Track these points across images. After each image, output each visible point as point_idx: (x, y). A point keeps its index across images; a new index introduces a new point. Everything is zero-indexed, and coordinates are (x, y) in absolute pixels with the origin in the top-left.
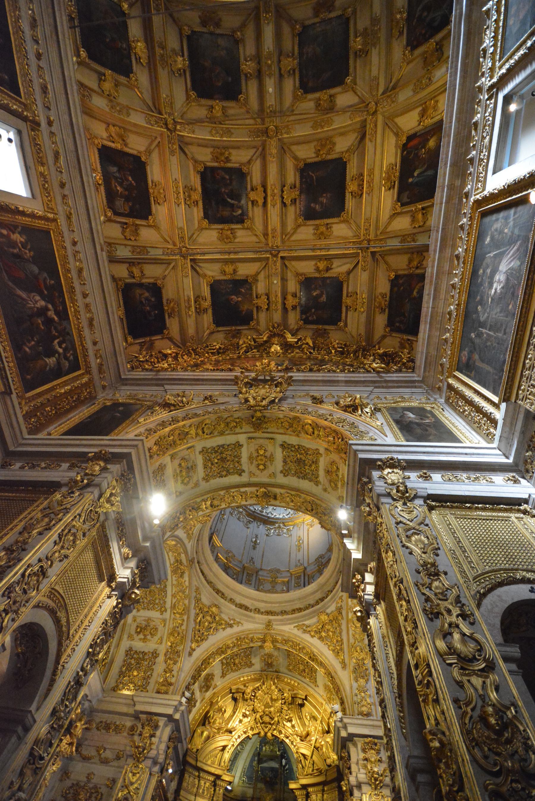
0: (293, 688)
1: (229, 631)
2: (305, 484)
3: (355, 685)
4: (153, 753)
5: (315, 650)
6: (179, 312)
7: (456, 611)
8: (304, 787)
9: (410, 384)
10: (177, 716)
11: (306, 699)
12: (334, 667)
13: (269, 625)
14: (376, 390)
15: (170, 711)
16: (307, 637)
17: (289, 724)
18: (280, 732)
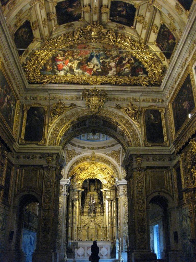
1: (79, 156)
3: (123, 171)
4: (64, 193)
5: (110, 160)
6: (39, 26)
7: (142, 202)
8: (106, 191)
9: (158, 92)
10: (68, 184)
11: (106, 168)
12: (116, 165)
13: (93, 153)
14: (143, 94)
15: (66, 183)
16: (107, 156)
17: (100, 175)
18: (97, 177)
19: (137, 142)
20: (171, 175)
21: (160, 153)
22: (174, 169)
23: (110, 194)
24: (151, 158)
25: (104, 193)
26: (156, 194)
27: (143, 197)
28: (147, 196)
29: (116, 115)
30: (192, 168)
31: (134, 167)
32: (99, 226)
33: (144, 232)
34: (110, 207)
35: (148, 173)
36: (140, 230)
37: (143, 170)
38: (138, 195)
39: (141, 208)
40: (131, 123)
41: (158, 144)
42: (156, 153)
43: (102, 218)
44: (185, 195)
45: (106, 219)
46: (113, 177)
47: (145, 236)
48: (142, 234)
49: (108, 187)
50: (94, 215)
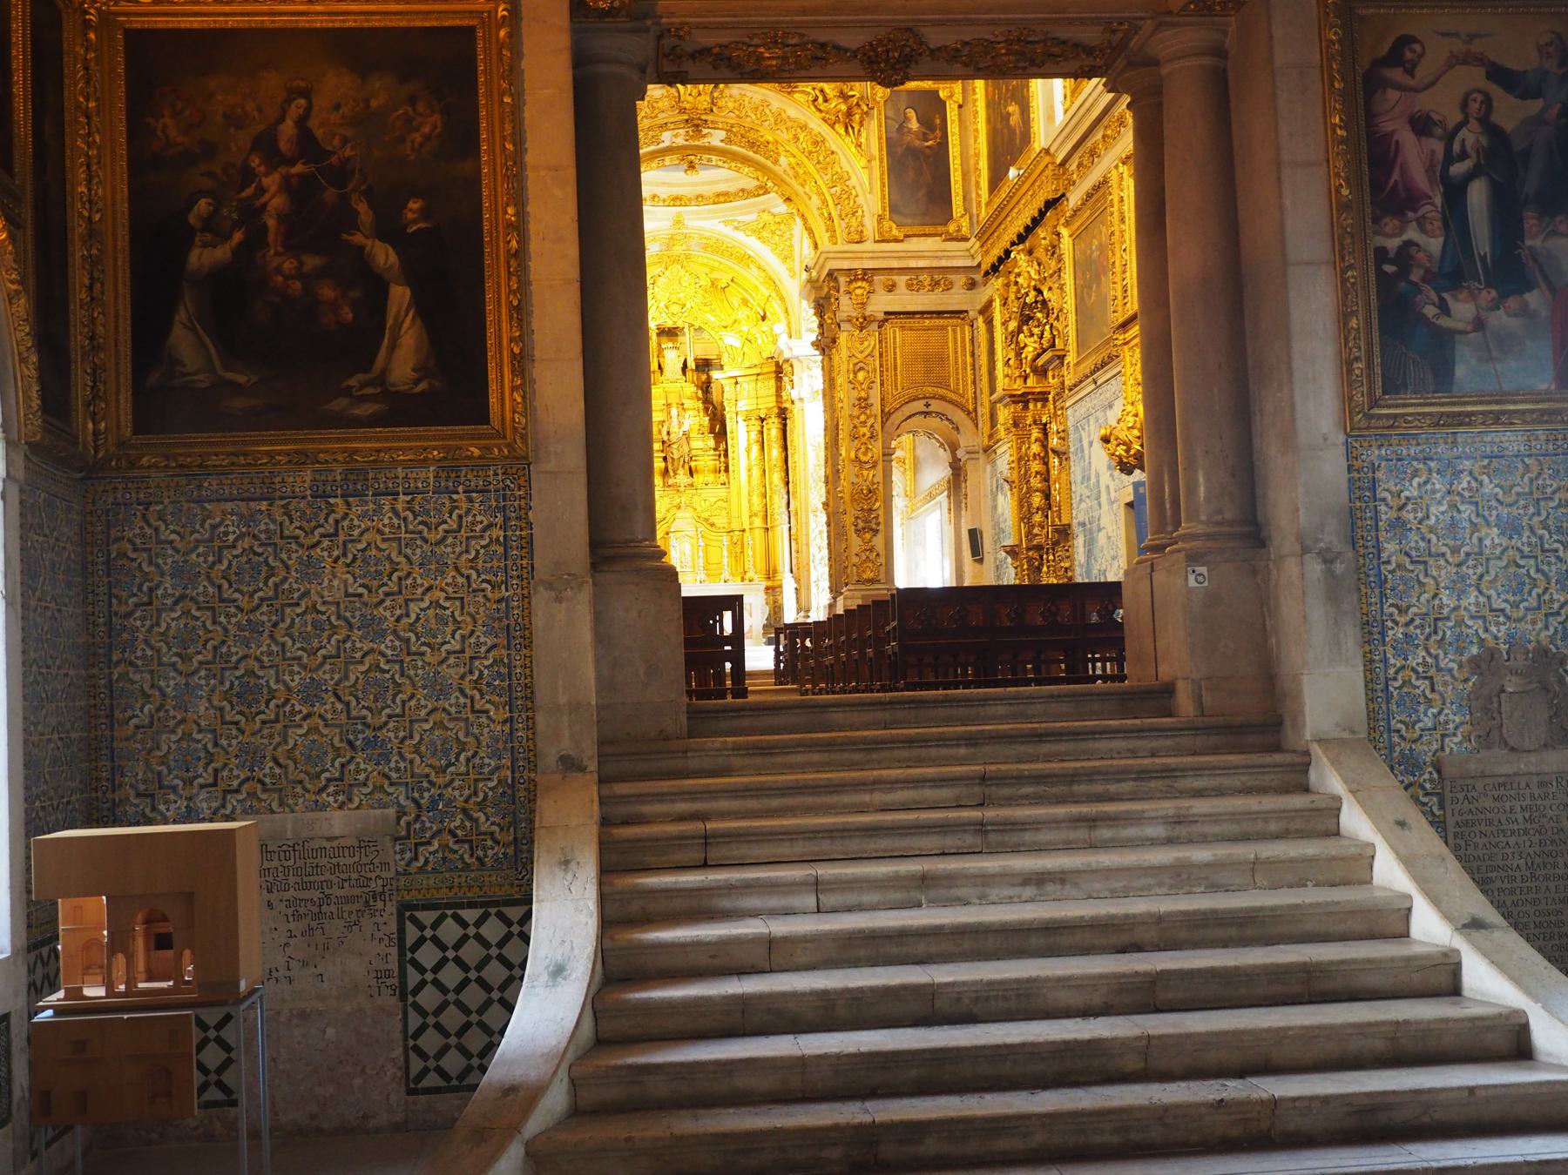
0: (712, 269)
2: (757, 157)
16: (740, 236)
19: (854, 223)
20: (972, 340)
21: (935, 264)
22: (981, 319)
23: (753, 393)
24: (901, 280)
25: (726, 389)
26: (919, 406)
27: (871, 421)
28: (886, 416)
29: (779, 119)
30: (1020, 331)
31: (841, 315)
32: (712, 525)
33: (877, 531)
34: (756, 448)
35: (893, 331)
36: (861, 525)
37: (875, 325)
38: (856, 412)
39: (865, 454)
40: (834, 148)
41: (928, 229)
42: (922, 263)
43: (722, 492)
44: (1004, 414)
45: (739, 494)
46: (763, 318)
47: (878, 541)
48: (868, 536)
49: (747, 364)
50: (690, 480)
